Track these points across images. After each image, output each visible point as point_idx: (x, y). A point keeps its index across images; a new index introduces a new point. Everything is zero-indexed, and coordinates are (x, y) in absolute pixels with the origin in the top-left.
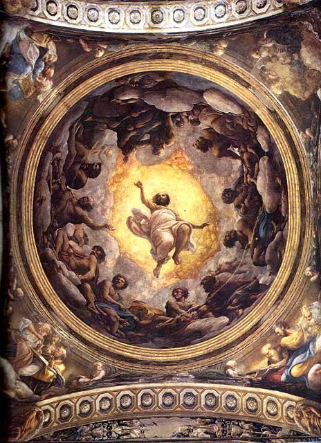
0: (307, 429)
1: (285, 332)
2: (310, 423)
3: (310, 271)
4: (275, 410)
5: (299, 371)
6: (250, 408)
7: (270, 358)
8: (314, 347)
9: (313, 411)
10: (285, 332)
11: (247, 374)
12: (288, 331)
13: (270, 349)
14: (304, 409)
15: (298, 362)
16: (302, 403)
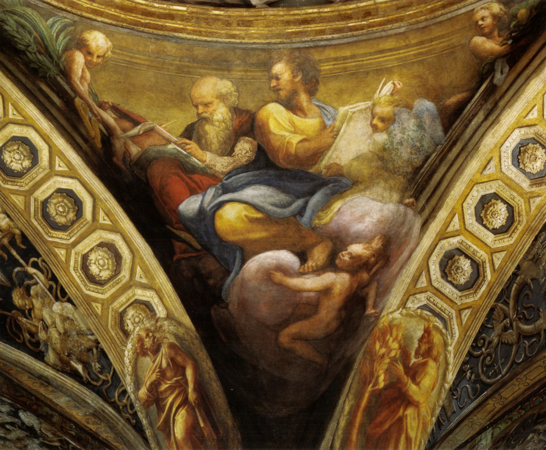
0: (138, 385)
1: (294, 93)
2: (154, 387)
3: (495, 17)
4: (105, 275)
5: (239, 225)
6: (52, 210)
7: (203, 120)
8: (326, 205)
9: (189, 373)
10: (294, 93)
11: (115, 109)
12: (303, 98)
13: (222, 97)
14: (172, 346)
15: (256, 201)
16: (181, 331)
